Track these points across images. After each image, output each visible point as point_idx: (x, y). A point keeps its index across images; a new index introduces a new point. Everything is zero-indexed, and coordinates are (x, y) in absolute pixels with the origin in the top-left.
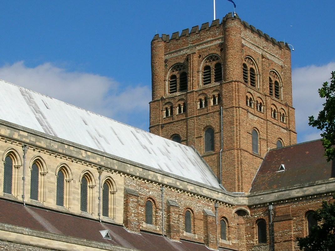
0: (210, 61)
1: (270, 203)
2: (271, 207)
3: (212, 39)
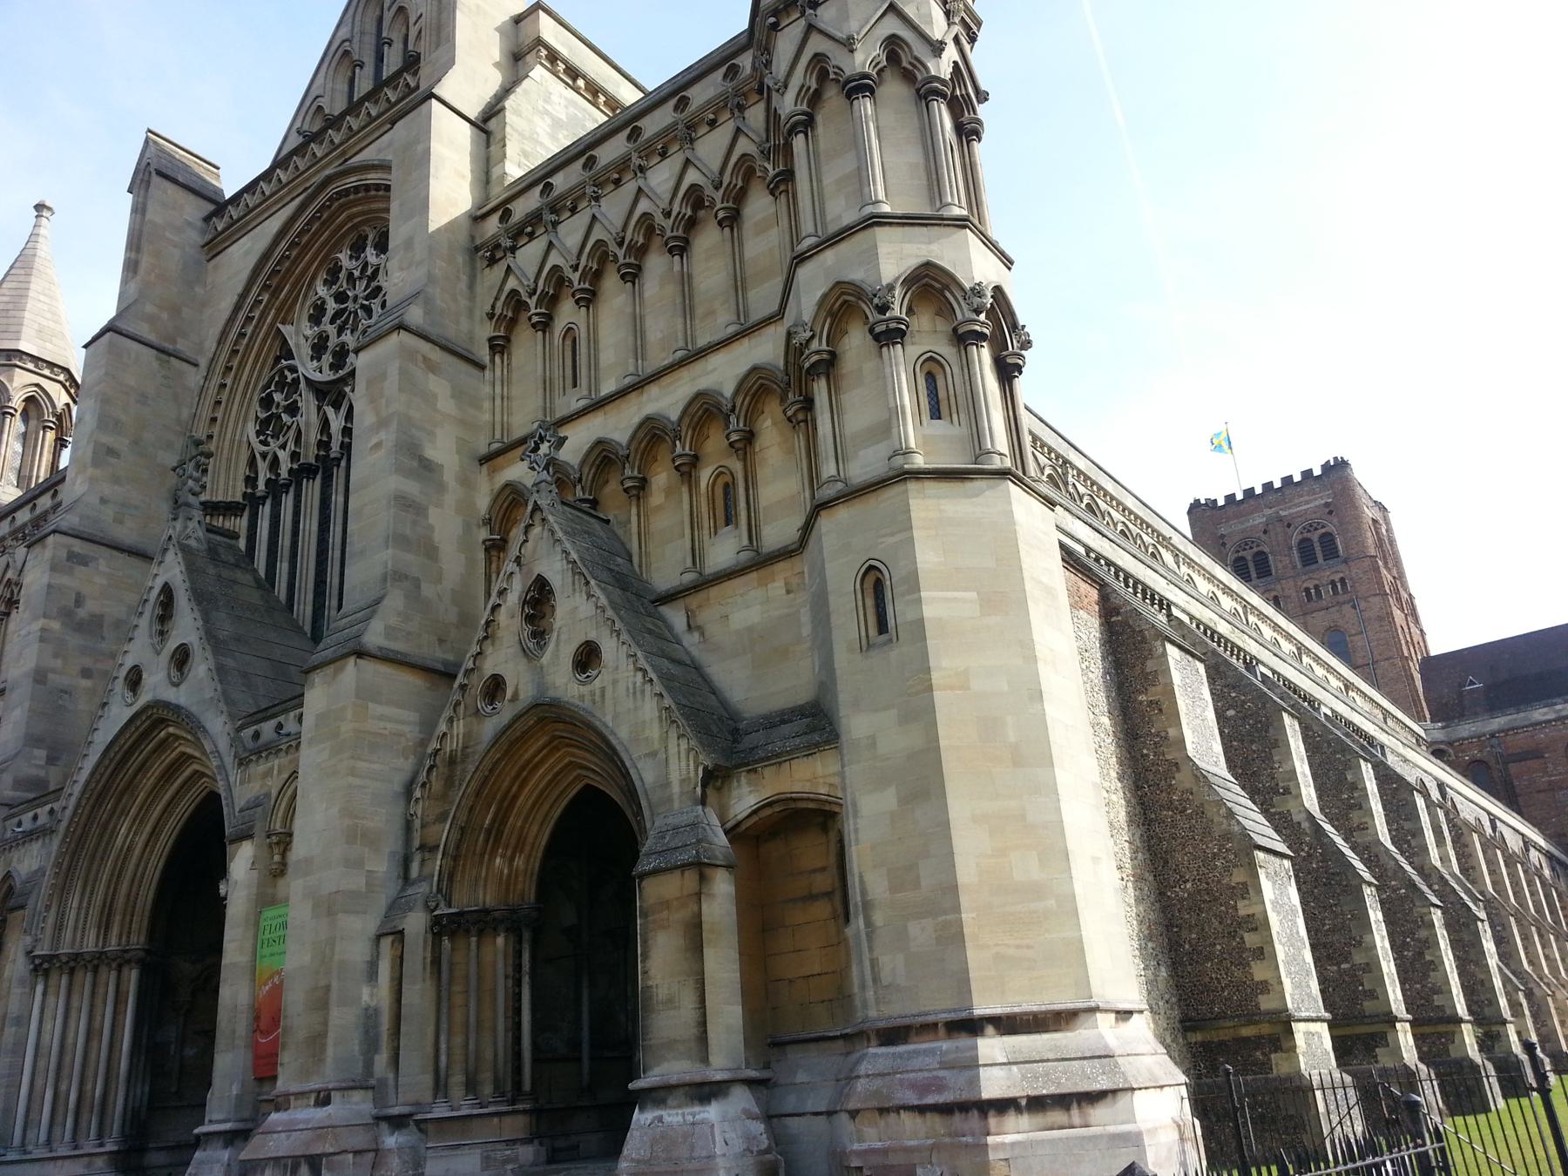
0: (1309, 531)
1: (1493, 735)
2: (1494, 741)
3: (1306, 498)
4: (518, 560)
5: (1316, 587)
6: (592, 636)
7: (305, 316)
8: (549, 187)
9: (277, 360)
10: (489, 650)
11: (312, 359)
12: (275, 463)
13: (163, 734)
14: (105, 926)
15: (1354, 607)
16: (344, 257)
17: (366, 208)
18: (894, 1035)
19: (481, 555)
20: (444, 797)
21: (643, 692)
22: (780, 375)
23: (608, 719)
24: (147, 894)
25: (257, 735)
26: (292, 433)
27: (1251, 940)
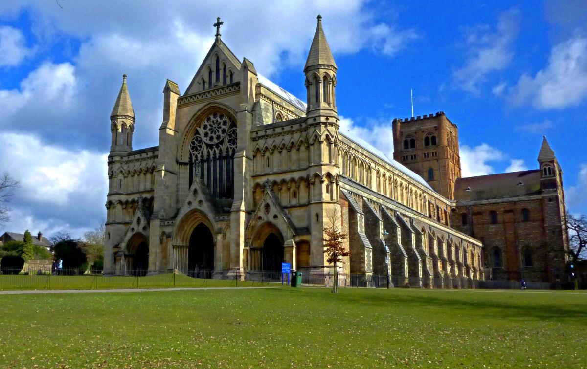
1: (470, 206)
2: (470, 208)
5: (428, 154)
6: (276, 214)
8: (266, 132)
10: (259, 212)
11: (205, 137)
12: (196, 157)
14: (183, 241)
15: (437, 161)
16: (212, 117)
18: (315, 268)
19: (252, 193)
23: (279, 226)
24: (189, 237)
25: (219, 218)
26: (200, 151)
27: (362, 260)
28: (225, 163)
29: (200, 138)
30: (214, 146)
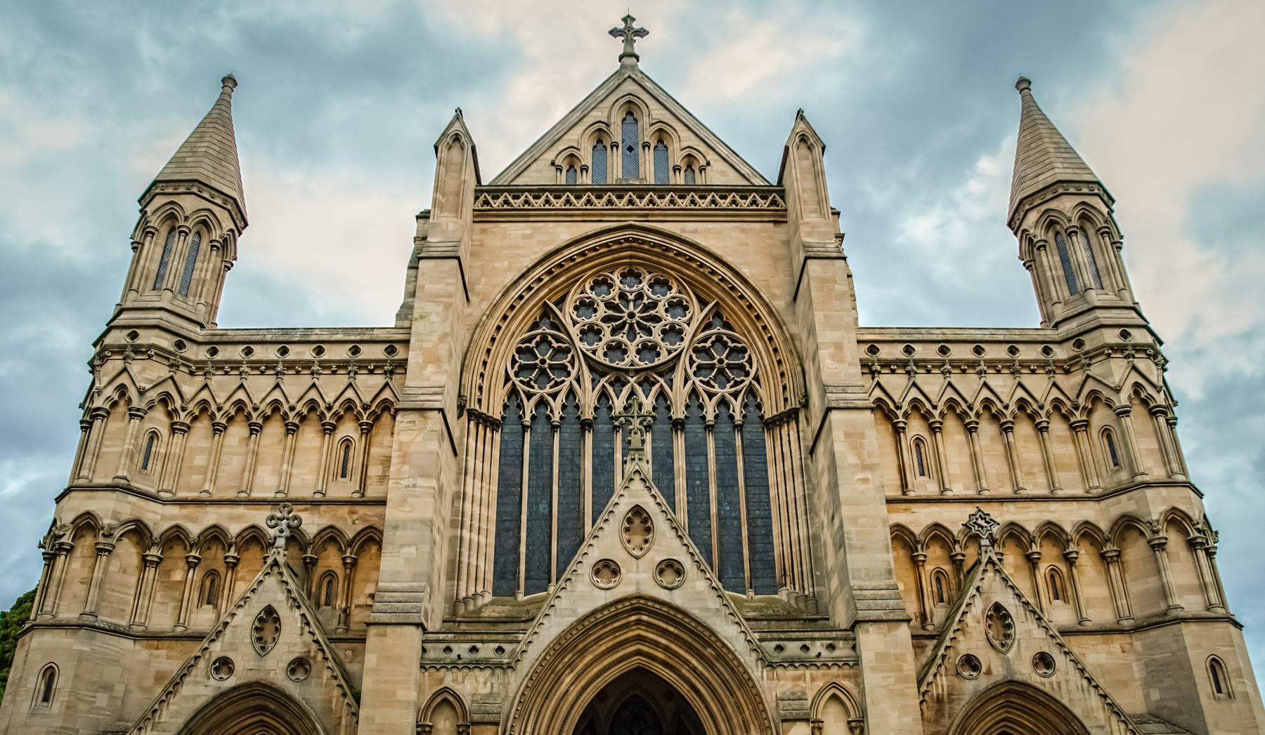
4: (978, 589)
6: (1046, 650)
7: (573, 305)
9: (535, 326)
13: (633, 618)
16: (616, 277)
17: (655, 258)
20: (936, 721)
21: (1089, 691)
22: (1106, 534)
23: (1065, 701)
26: (564, 388)
28: (679, 443)
29: (558, 340)
30: (632, 380)
